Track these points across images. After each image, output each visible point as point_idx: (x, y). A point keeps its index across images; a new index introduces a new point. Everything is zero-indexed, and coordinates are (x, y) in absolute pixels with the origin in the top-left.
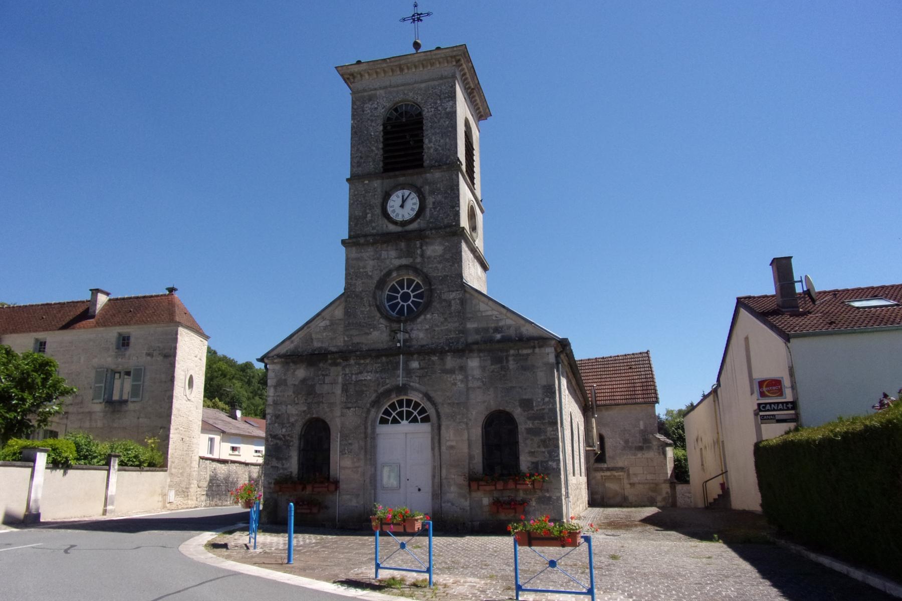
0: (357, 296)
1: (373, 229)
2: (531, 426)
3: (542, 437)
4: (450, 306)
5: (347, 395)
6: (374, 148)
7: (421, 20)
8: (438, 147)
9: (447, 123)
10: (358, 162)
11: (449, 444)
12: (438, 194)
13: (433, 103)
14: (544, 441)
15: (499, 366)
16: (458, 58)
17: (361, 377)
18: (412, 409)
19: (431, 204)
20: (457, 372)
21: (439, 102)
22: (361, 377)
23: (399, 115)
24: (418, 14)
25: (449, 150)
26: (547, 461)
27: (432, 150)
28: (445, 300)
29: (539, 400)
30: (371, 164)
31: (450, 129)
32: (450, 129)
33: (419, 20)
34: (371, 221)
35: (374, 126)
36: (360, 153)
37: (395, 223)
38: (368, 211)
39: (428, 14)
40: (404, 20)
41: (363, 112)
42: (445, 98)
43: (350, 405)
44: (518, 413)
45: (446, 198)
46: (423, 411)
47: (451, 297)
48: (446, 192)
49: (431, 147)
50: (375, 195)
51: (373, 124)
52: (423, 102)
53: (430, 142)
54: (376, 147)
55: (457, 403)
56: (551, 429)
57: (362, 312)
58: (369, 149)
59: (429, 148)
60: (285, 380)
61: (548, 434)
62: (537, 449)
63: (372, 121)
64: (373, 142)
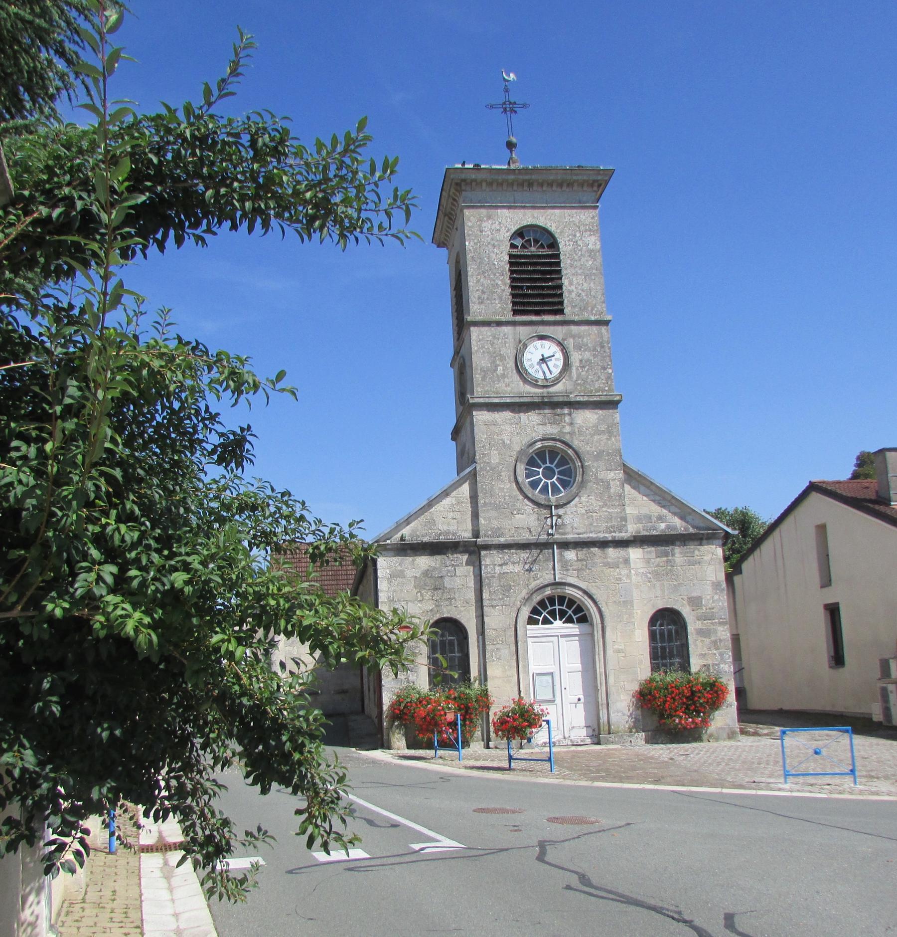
0: (493, 469)
1: (506, 386)
2: (700, 626)
3: (713, 639)
4: (608, 487)
5: (490, 592)
6: (500, 283)
7: (516, 112)
8: (580, 292)
9: (590, 263)
10: (479, 298)
11: (616, 647)
12: (586, 350)
13: (572, 235)
14: (715, 642)
15: (665, 559)
16: (600, 182)
17: (505, 569)
18: (566, 607)
19: (578, 361)
20: (621, 566)
21: (578, 235)
22: (505, 569)
23: (525, 242)
24: (510, 103)
25: (594, 297)
26: (718, 665)
27: (573, 295)
28: (602, 480)
29: (708, 597)
30: (497, 302)
31: (594, 271)
32: (594, 271)
33: (513, 111)
34: (504, 376)
35: (497, 254)
36: (482, 286)
37: (534, 383)
38: (498, 362)
39: (524, 106)
40: (492, 107)
41: (481, 232)
42: (586, 231)
43: (495, 603)
44: (686, 612)
45: (595, 356)
46: (579, 609)
47: (610, 477)
48: (594, 350)
49: (573, 291)
50: (505, 342)
51: (496, 250)
52: (558, 231)
53: (571, 283)
54: (502, 281)
55: (624, 601)
56: (722, 629)
57: (501, 489)
58: (492, 282)
59: (570, 292)
60: (402, 572)
61: (719, 634)
62: (707, 652)
63: (494, 246)
64: (497, 275)
